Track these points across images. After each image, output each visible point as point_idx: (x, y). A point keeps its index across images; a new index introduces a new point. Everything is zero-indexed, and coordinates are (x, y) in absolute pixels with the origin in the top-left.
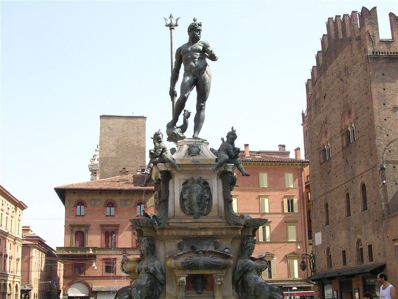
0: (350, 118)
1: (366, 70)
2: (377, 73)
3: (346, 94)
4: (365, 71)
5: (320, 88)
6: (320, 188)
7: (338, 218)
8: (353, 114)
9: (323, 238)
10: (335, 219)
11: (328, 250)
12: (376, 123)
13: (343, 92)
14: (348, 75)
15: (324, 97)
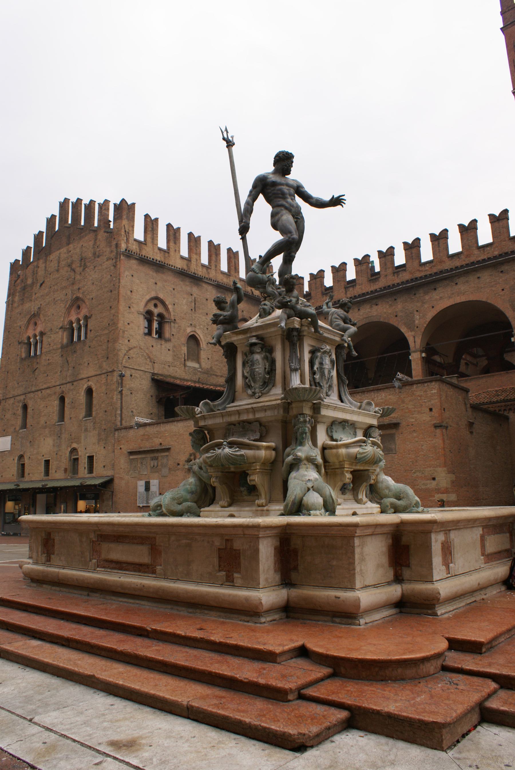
0: (78, 313)
1: (114, 266)
2: (127, 273)
3: (77, 287)
4: (112, 268)
5: (35, 273)
6: (17, 385)
7: (42, 422)
8: (84, 311)
9: (13, 444)
10: (38, 423)
11: (21, 457)
12: (120, 325)
13: (73, 284)
14: (85, 267)
15: (41, 285)
